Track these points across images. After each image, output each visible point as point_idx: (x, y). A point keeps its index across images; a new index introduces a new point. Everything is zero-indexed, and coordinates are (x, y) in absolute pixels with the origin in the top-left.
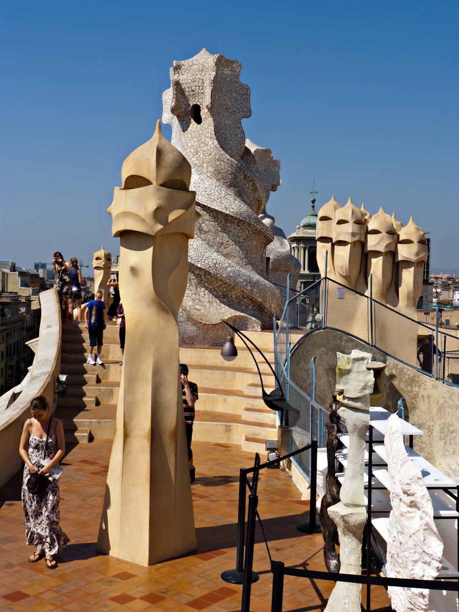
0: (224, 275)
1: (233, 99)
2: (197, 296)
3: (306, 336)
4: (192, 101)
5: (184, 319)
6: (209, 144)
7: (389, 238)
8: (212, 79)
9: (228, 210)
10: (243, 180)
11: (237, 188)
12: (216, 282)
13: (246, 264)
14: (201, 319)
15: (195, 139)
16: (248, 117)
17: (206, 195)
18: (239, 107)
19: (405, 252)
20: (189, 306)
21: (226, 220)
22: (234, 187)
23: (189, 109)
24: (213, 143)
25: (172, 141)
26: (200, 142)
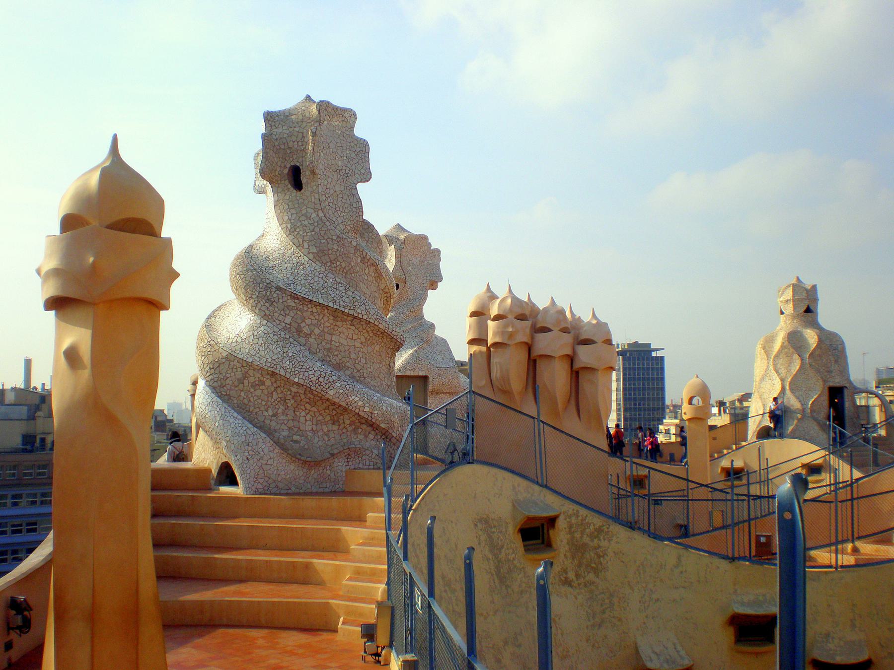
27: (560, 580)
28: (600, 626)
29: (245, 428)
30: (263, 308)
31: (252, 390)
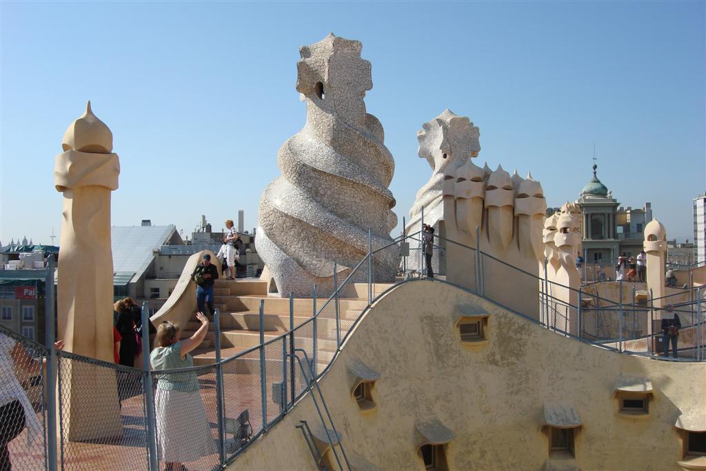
27: (488, 360)
28: (517, 393)
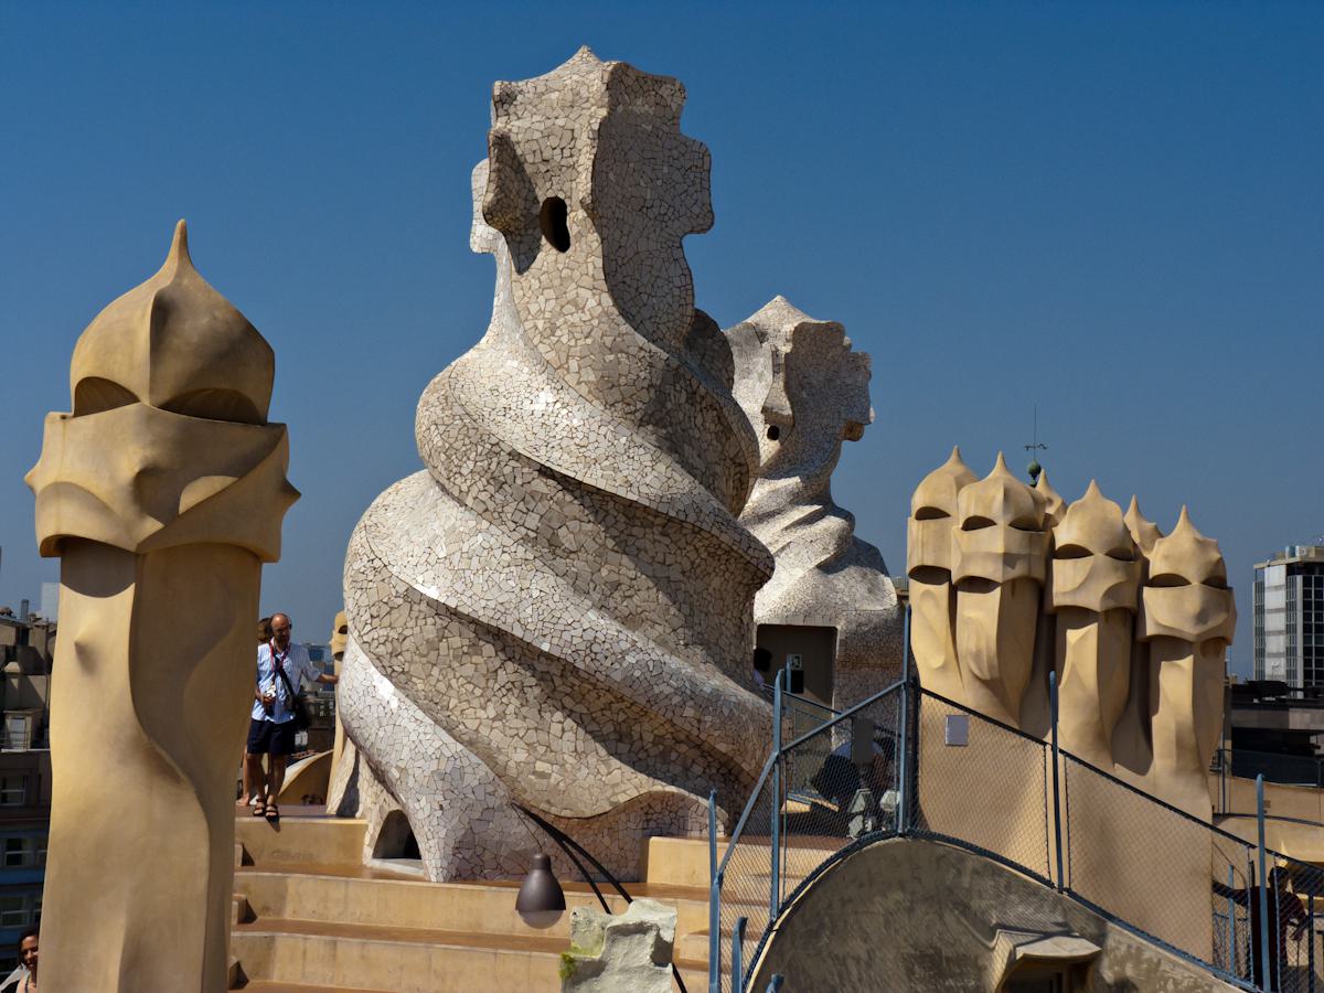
0: (617, 676)
1: (659, 182)
2: (543, 736)
3: (843, 854)
4: (544, 189)
5: (498, 802)
6: (589, 305)
7: (1116, 569)
8: (596, 127)
9: (635, 490)
10: (687, 406)
11: (665, 427)
12: (594, 694)
13: (686, 645)
14: (548, 802)
15: (550, 293)
16: (704, 231)
17: (573, 448)
18: (677, 202)
19: (1162, 611)
20: (518, 764)
21: (630, 520)
22: (654, 425)
23: (536, 210)
24: (597, 303)
25: (496, 299)
26: (563, 301)
29: (437, 744)
30: (484, 496)
31: (455, 665)
